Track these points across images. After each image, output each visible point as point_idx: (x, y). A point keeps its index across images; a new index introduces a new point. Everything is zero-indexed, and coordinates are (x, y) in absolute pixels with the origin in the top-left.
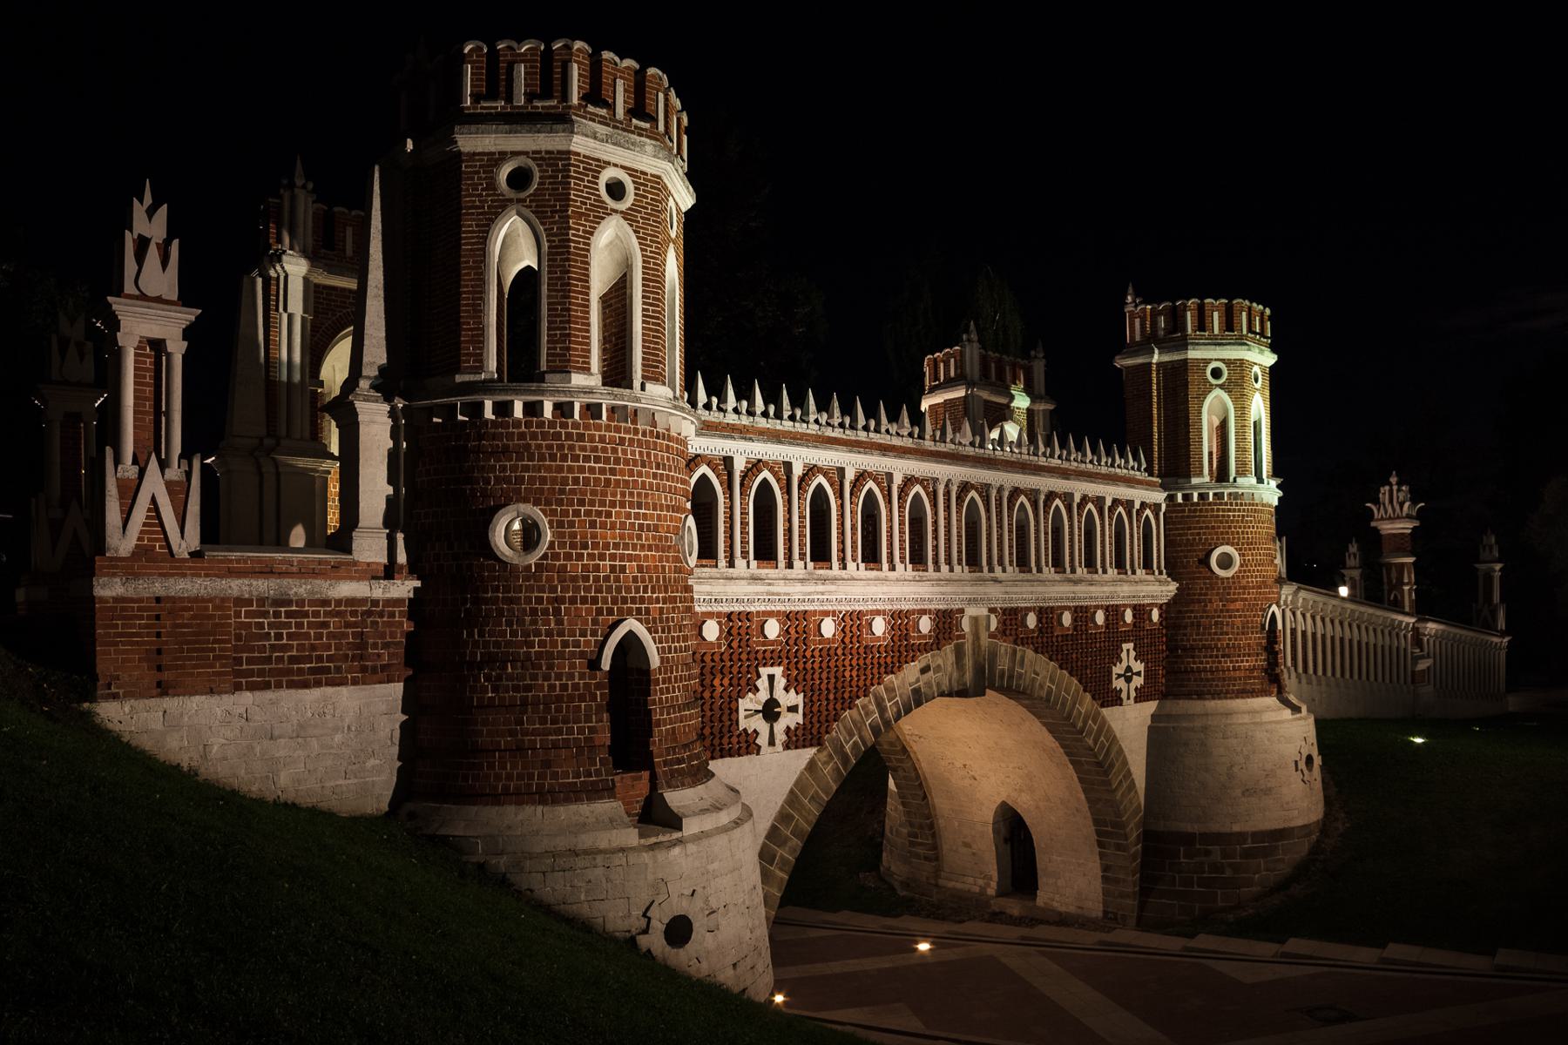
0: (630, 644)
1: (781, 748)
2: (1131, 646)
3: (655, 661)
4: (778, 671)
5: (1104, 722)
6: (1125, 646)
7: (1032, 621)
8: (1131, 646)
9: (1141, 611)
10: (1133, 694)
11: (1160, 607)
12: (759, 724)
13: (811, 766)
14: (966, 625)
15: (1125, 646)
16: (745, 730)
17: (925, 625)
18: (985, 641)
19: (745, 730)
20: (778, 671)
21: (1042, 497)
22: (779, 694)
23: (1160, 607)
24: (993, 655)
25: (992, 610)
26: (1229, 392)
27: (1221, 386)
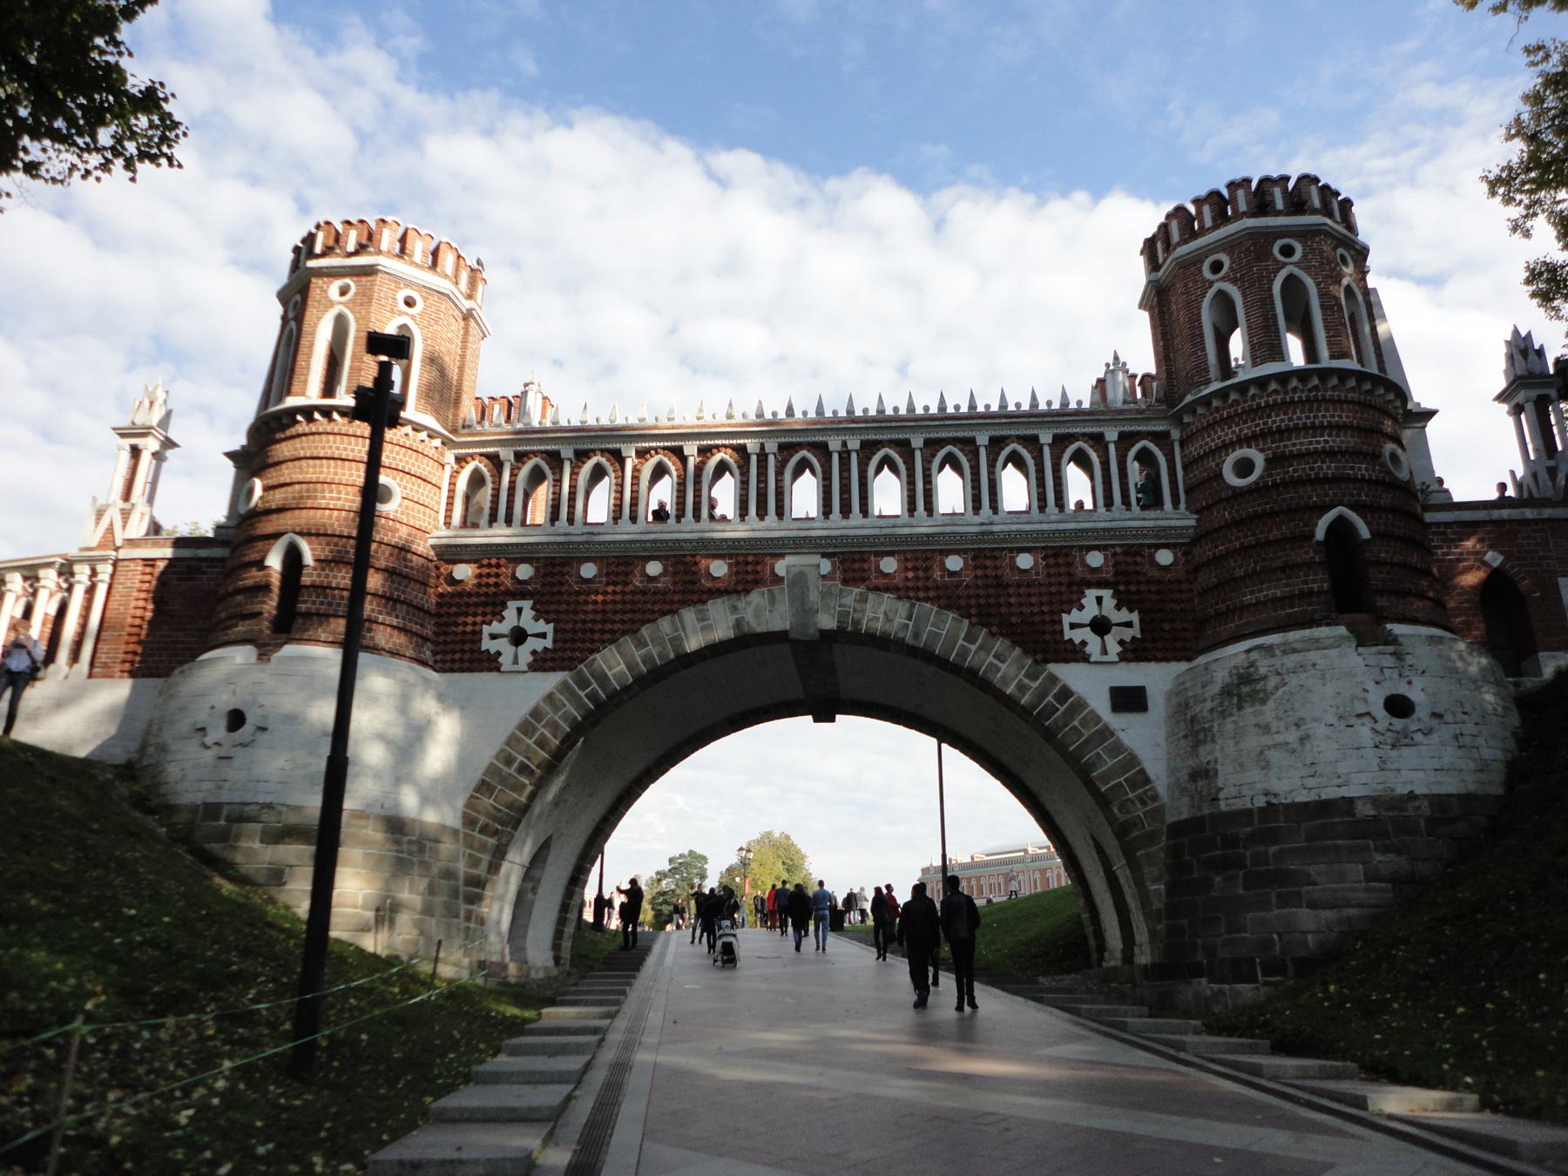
1: (526, 669)
3: (308, 559)
4: (527, 605)
5: (1053, 679)
8: (1106, 594)
10: (1114, 649)
12: (504, 646)
13: (564, 687)
16: (488, 651)
17: (719, 568)
19: (488, 651)
20: (527, 605)
25: (824, 555)
26: (1234, 281)
27: (1222, 279)
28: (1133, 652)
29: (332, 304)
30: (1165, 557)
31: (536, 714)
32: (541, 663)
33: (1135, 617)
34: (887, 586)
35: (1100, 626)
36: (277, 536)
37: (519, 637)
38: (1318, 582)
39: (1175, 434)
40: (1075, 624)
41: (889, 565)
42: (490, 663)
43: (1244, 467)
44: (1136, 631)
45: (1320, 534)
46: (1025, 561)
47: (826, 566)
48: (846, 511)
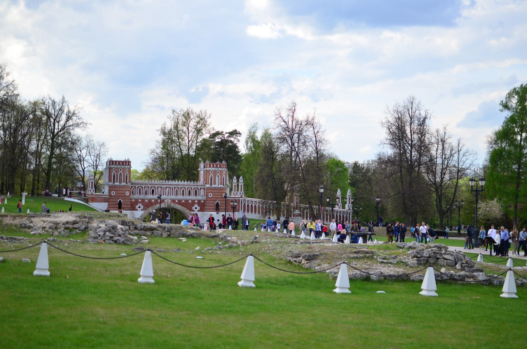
0: (120, 201)
2: (197, 205)
3: (122, 202)
6: (195, 205)
7: (177, 201)
8: (197, 205)
9: (199, 201)
11: (204, 200)
13: (144, 212)
14: (166, 201)
15: (195, 205)
18: (169, 203)
20: (140, 204)
21: (180, 188)
22: (140, 206)
23: (204, 200)
24: (170, 204)
28: (198, 211)
29: (120, 171)
30: (202, 201)
31: (142, 215)
32: (142, 210)
33: (199, 207)
34: (176, 203)
35: (196, 208)
36: (118, 199)
37: (139, 207)
38: (215, 207)
39: (206, 188)
40: (194, 208)
41: (177, 201)
42: (137, 210)
43: (210, 195)
44: (199, 209)
45: (216, 203)
46: (190, 201)
47: (170, 201)
48: (172, 195)
